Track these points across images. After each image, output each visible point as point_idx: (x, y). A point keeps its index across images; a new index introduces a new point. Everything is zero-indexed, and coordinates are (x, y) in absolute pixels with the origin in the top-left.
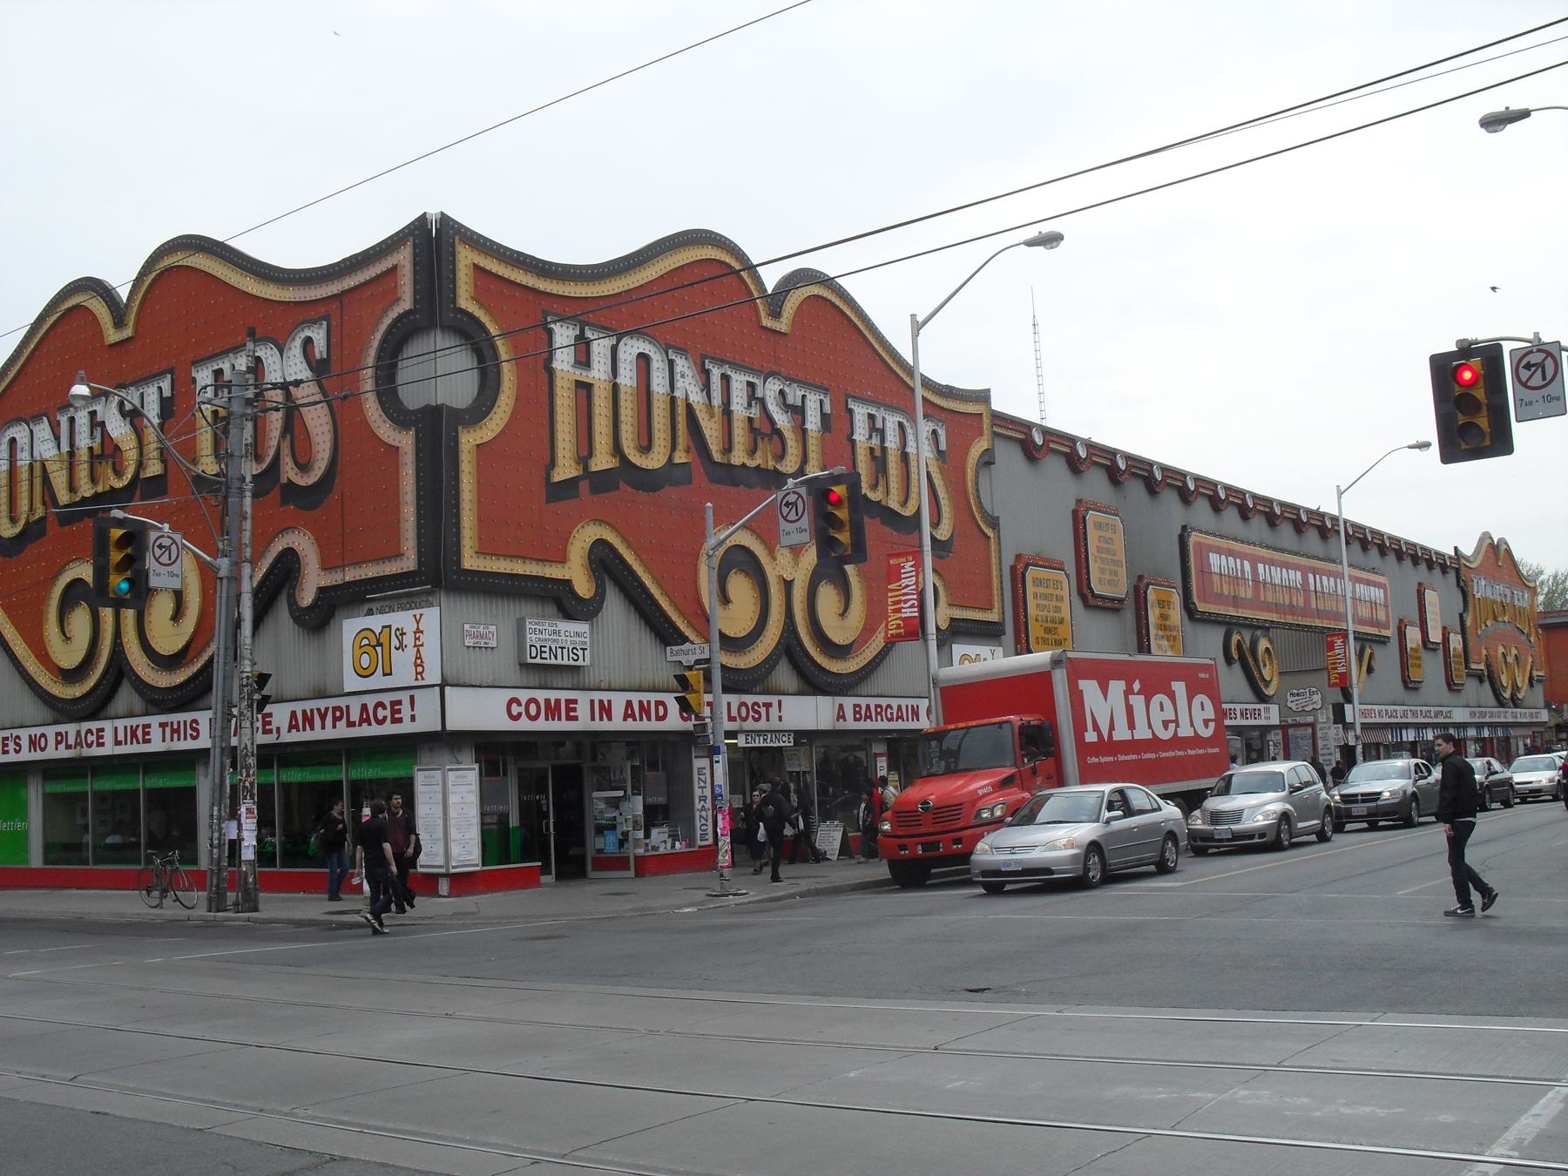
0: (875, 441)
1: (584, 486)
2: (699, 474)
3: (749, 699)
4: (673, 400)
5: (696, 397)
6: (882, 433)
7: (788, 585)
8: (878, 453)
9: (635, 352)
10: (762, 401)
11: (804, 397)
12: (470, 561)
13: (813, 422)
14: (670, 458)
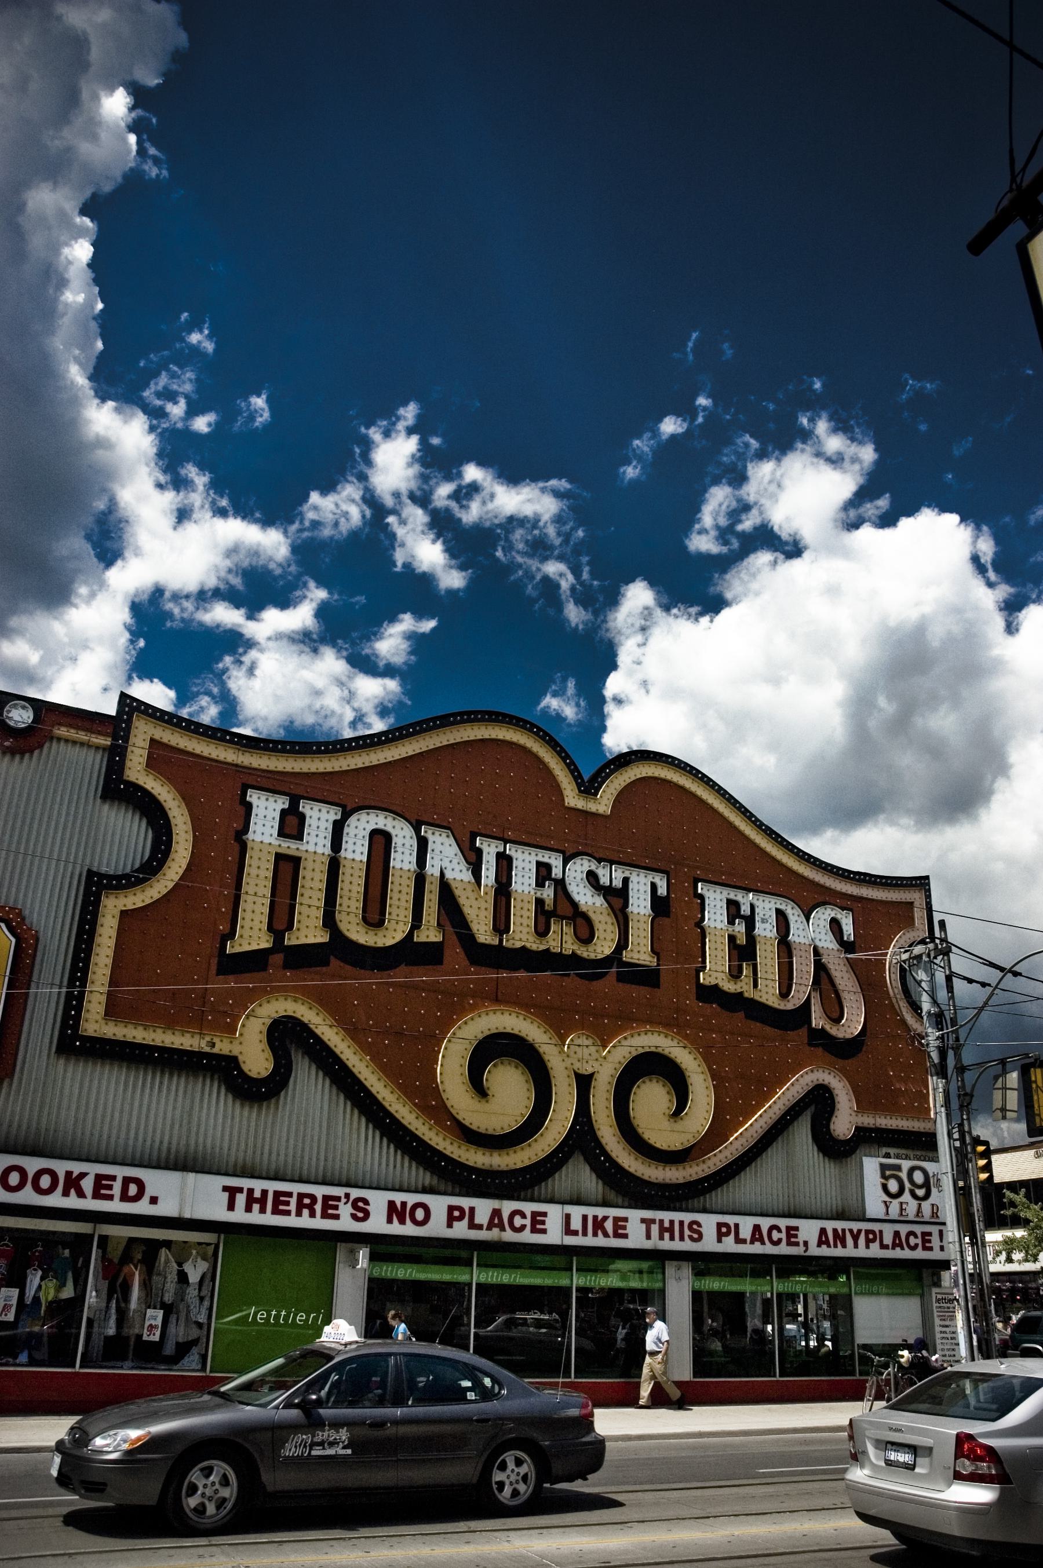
0: (740, 928)
1: (278, 959)
2: (455, 955)
3: (508, 1207)
4: (420, 879)
5: (459, 873)
6: (750, 922)
7: (584, 1083)
8: (742, 940)
9: (371, 827)
10: (561, 885)
11: (626, 881)
12: (95, 1023)
13: (640, 904)
14: (411, 934)
